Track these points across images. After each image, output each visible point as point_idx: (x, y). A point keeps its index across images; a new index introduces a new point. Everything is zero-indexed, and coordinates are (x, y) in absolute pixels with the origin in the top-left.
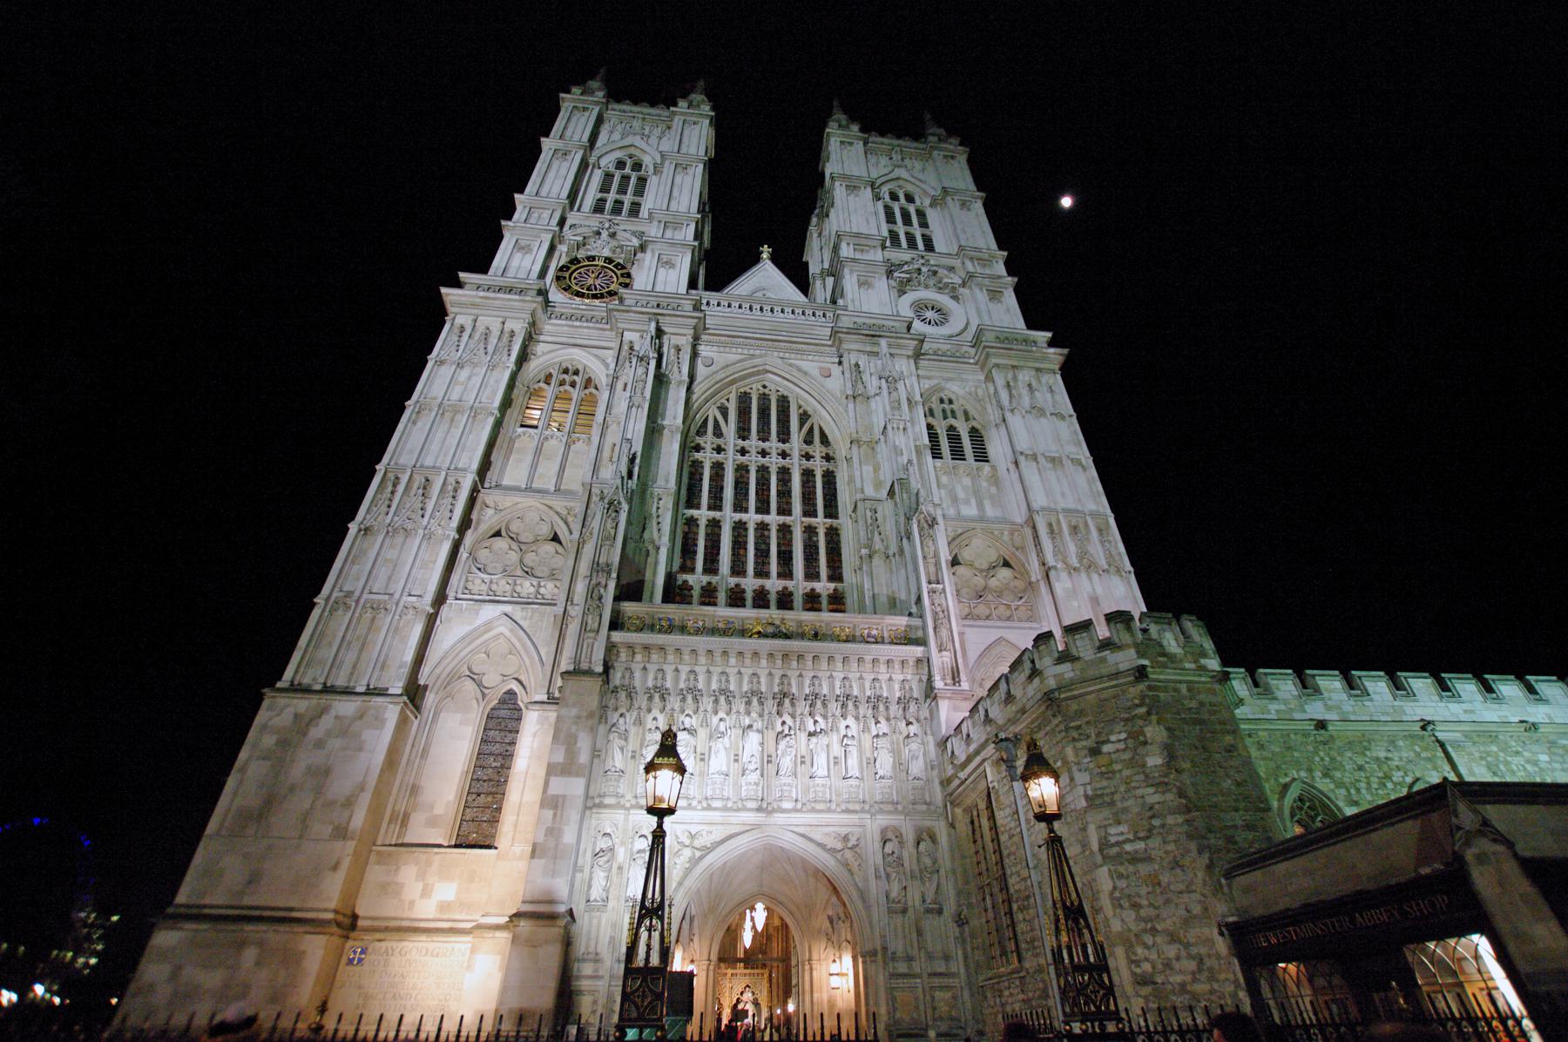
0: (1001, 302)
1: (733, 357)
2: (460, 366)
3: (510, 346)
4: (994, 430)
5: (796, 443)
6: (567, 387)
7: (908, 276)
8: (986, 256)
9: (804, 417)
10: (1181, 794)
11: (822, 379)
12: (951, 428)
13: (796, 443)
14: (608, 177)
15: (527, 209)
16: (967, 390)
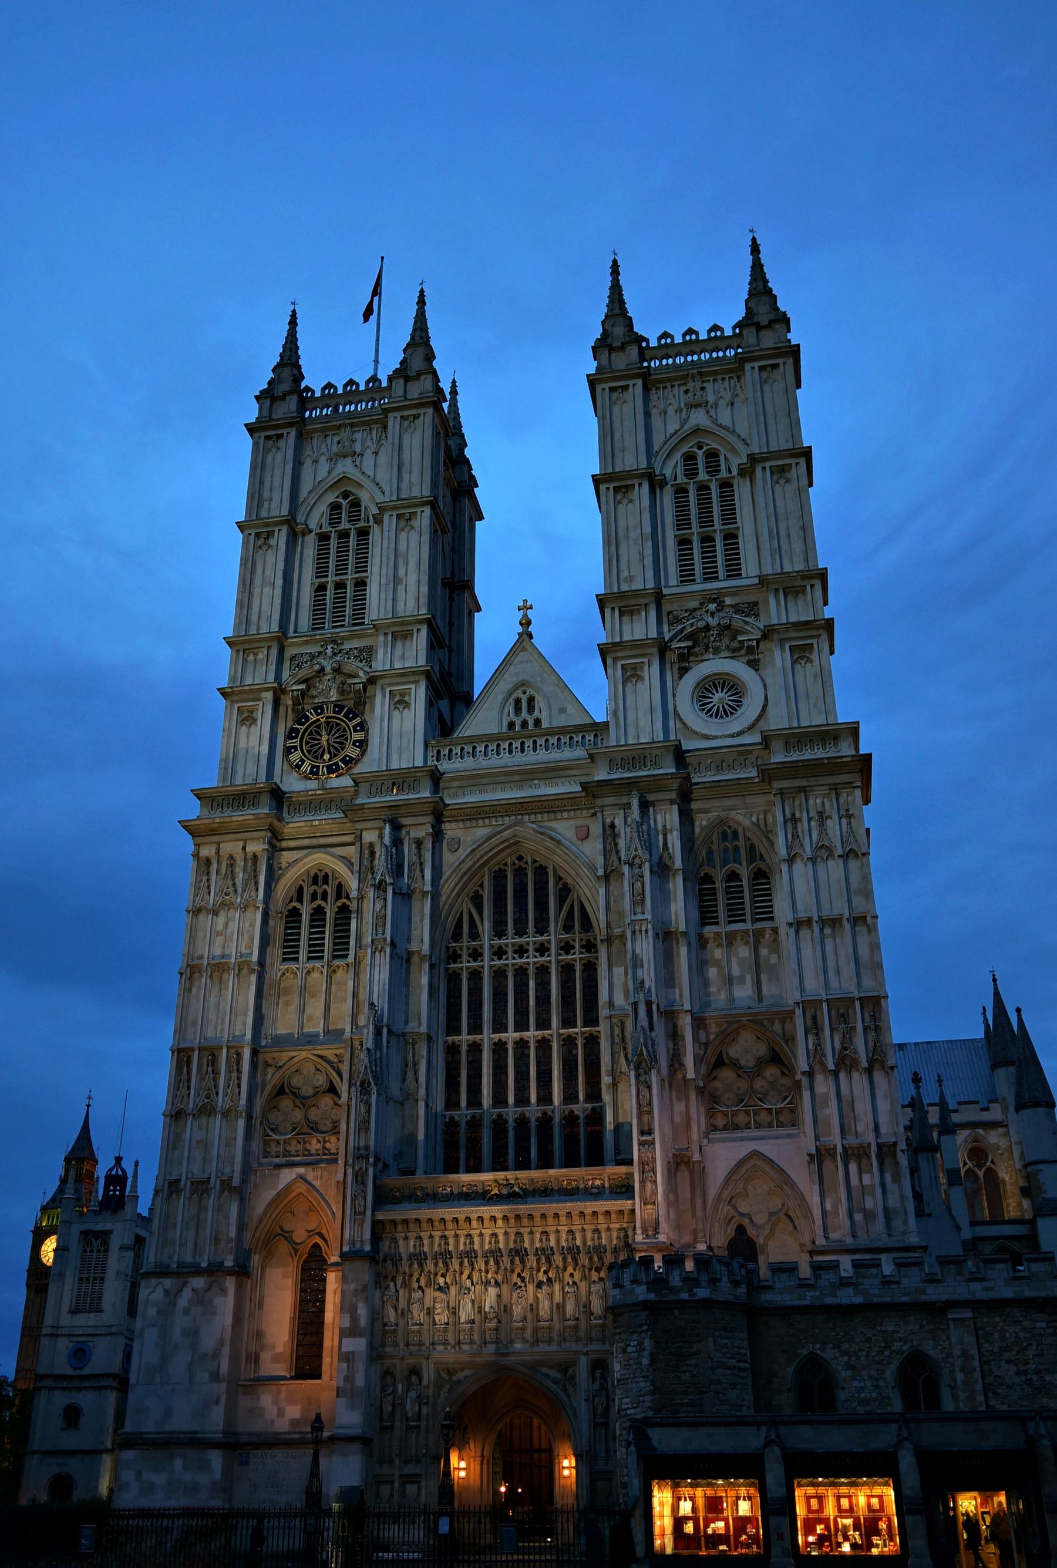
0: (810, 660)
1: (481, 832)
2: (216, 913)
3: (255, 877)
4: (778, 876)
5: (554, 936)
6: (319, 902)
7: (690, 643)
8: (799, 583)
9: (565, 891)
10: (653, 1384)
11: (579, 842)
12: (733, 876)
13: (554, 936)
14: (324, 538)
15: (241, 654)
16: (754, 819)
